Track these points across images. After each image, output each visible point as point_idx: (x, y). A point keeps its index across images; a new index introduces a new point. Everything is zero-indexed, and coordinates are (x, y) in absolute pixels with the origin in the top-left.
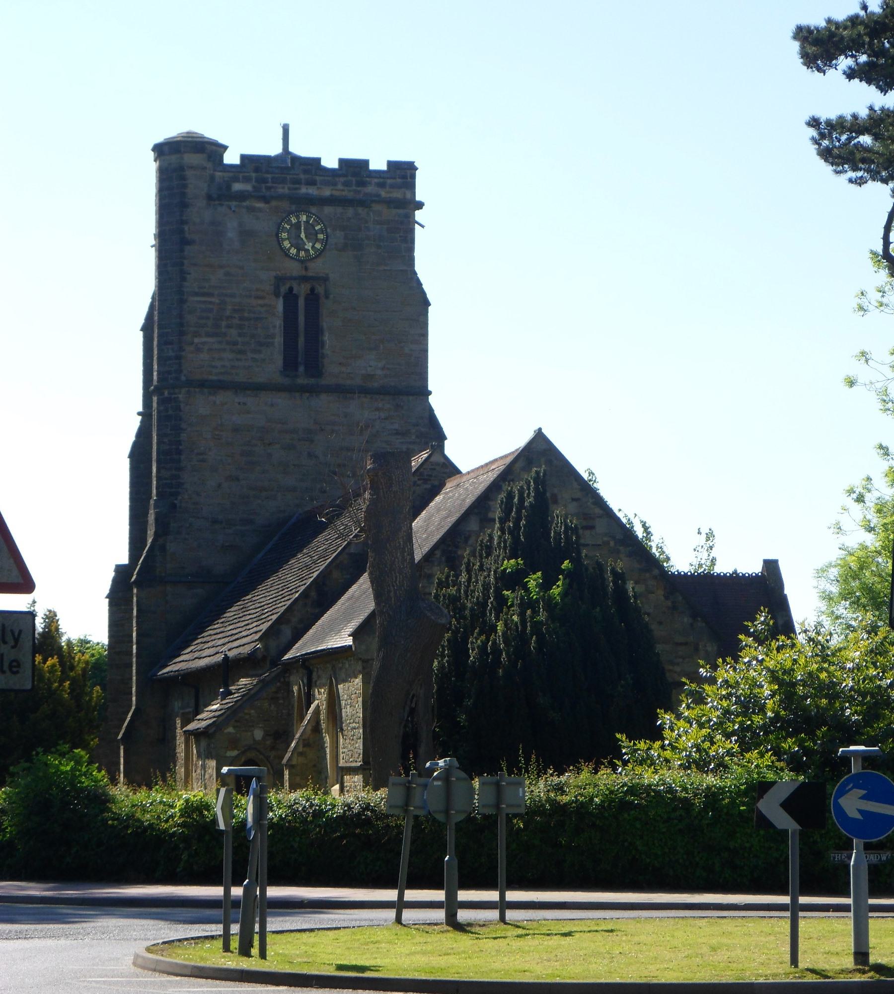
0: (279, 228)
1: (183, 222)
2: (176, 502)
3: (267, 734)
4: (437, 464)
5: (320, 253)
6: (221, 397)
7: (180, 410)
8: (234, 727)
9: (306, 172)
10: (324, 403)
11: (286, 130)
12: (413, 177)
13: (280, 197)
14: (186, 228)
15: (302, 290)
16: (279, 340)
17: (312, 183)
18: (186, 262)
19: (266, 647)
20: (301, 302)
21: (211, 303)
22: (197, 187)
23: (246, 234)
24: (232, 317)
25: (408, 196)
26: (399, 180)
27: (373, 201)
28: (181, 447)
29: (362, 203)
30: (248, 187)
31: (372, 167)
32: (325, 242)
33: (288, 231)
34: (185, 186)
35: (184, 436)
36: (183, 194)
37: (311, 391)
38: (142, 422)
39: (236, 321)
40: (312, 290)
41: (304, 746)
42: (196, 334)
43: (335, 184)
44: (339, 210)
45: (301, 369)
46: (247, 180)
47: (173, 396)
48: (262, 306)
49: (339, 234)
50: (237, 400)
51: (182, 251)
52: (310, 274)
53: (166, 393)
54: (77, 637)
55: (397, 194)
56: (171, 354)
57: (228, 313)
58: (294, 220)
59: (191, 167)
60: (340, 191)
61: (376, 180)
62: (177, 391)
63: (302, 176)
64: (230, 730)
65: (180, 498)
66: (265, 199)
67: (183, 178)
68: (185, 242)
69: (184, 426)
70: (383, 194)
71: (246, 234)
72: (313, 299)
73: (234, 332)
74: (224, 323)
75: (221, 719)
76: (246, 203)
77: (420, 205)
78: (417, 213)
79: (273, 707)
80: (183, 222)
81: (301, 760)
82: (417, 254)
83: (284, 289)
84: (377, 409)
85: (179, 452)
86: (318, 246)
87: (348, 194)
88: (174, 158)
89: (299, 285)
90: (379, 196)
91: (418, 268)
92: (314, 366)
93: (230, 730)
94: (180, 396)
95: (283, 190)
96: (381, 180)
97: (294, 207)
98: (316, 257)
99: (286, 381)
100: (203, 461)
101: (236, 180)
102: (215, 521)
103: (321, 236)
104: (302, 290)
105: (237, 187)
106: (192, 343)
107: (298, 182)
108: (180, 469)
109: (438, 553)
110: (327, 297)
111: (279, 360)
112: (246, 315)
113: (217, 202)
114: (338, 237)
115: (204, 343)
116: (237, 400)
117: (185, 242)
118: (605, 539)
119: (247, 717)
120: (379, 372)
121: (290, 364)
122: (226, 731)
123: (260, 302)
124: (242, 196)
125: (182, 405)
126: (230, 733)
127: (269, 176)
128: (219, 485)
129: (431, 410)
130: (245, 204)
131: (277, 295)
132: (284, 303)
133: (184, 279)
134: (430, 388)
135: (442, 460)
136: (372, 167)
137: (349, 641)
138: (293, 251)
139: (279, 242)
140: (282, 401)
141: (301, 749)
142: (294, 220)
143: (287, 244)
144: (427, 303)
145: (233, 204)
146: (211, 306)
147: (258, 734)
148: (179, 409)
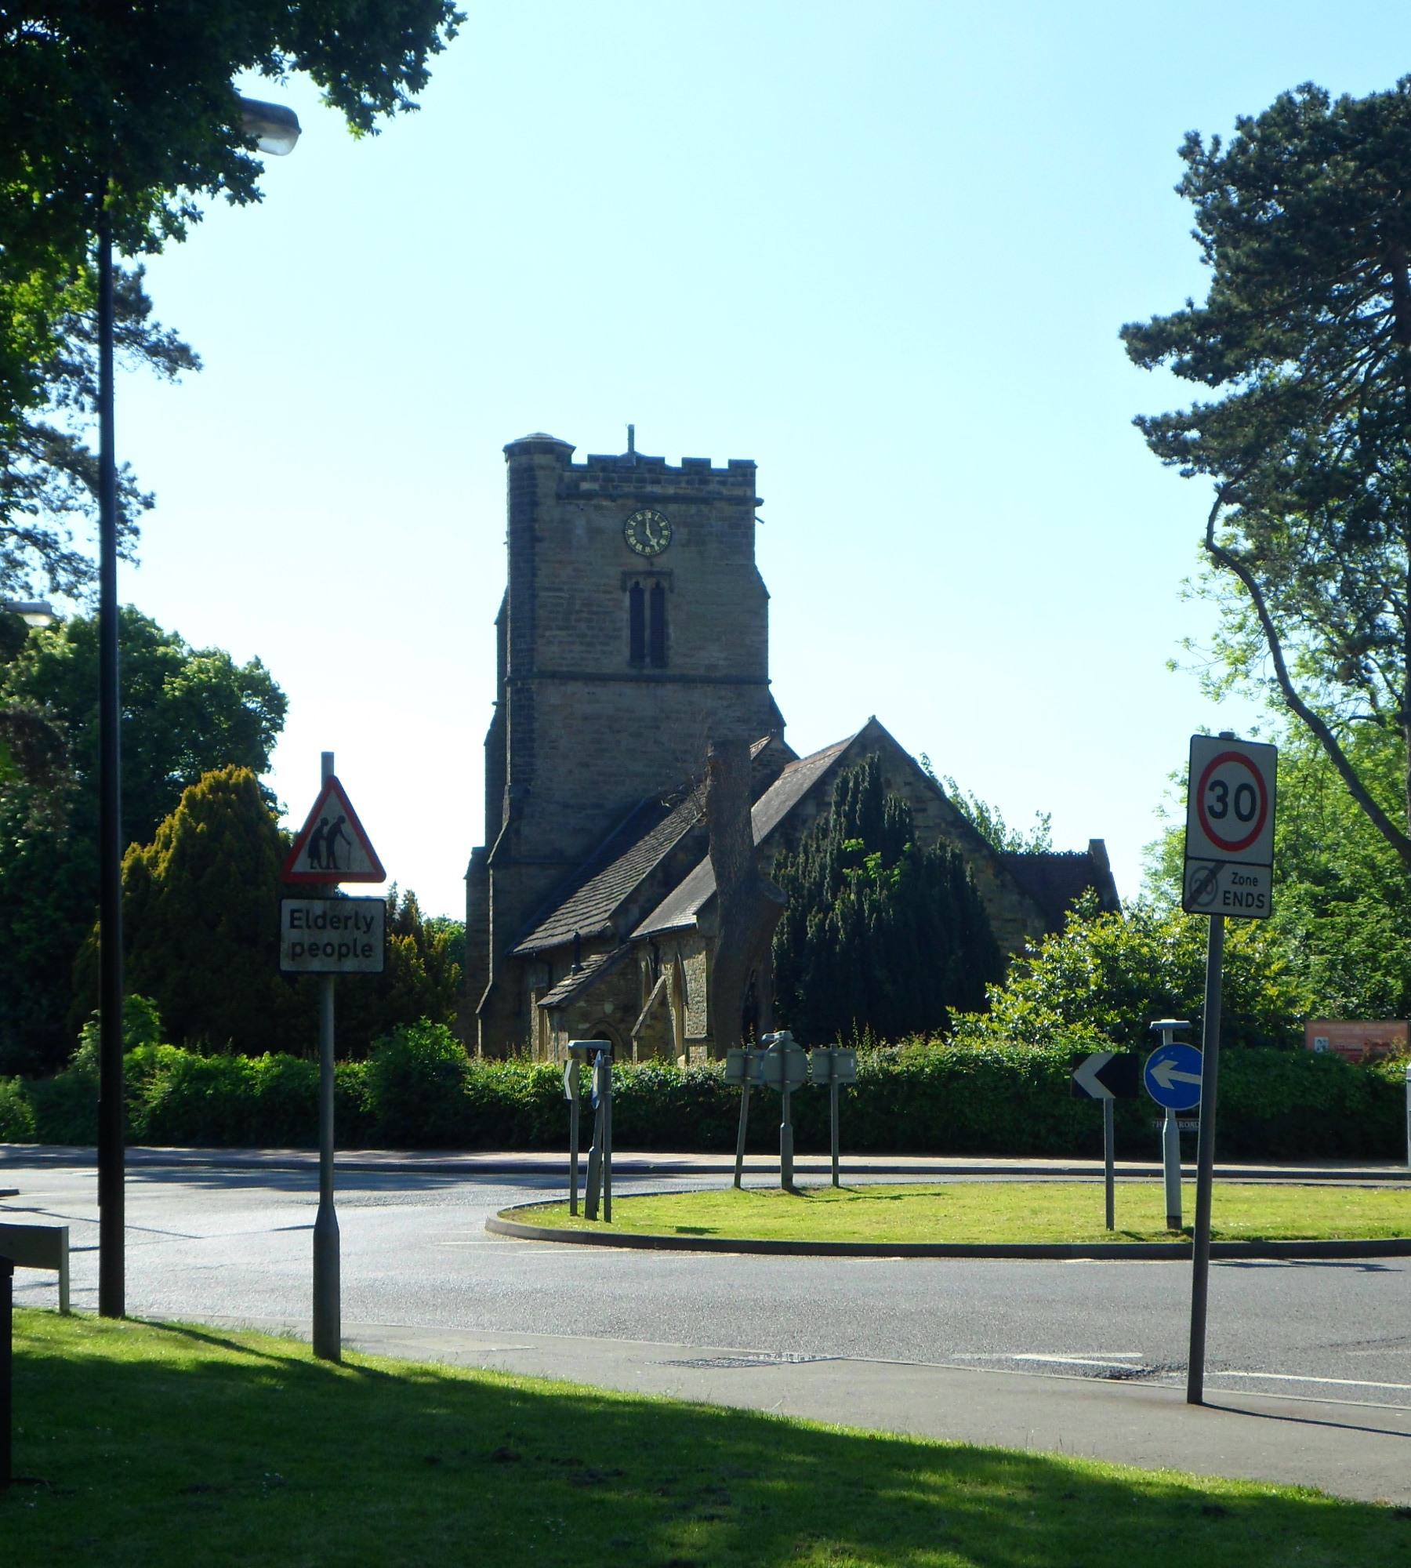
0: (625, 525)
1: (534, 520)
2: (529, 787)
3: (617, 1008)
4: (777, 750)
5: (664, 549)
6: (572, 687)
7: (533, 700)
8: (586, 1001)
9: (650, 471)
10: (671, 694)
11: (631, 431)
12: (753, 475)
13: (626, 496)
14: (537, 526)
15: (647, 584)
16: (626, 633)
17: (657, 482)
18: (537, 559)
19: (615, 925)
20: (647, 597)
21: (562, 598)
22: (547, 485)
23: (594, 532)
24: (582, 611)
25: (749, 493)
26: (740, 479)
27: (715, 499)
28: (534, 736)
29: (705, 501)
30: (595, 486)
31: (713, 466)
32: (670, 539)
33: (634, 528)
34: (535, 486)
35: (536, 725)
36: (534, 493)
37: (659, 681)
38: (496, 711)
39: (585, 615)
40: (658, 584)
41: (652, 1019)
43: (679, 483)
44: (683, 507)
45: (648, 660)
46: (594, 479)
47: (527, 687)
48: (609, 600)
49: (684, 530)
50: (586, 690)
51: (533, 548)
52: (655, 569)
53: (519, 684)
54: (436, 917)
55: (738, 492)
56: (524, 646)
57: (577, 607)
58: (639, 517)
59: (542, 467)
60: (684, 489)
61: (718, 478)
62: (530, 681)
63: (647, 476)
64: (582, 1004)
65: (533, 783)
66: (612, 498)
67: (533, 478)
68: (536, 539)
69: (536, 715)
70: (725, 491)
71: (594, 532)
72: (658, 593)
73: (583, 626)
74: (573, 617)
75: (573, 993)
76: (594, 502)
77: (760, 502)
78: (757, 509)
79: (622, 982)
80: (534, 520)
81: (650, 1032)
82: (757, 549)
83: (630, 584)
84: (721, 698)
85: (532, 740)
86: (663, 542)
87: (690, 492)
88: (524, 459)
89: (645, 579)
90: (719, 493)
91: (757, 563)
92: (660, 655)
93: (582, 1004)
94: (533, 687)
95: (629, 488)
96: (722, 479)
97: (639, 505)
98: (661, 552)
99: (634, 672)
100: (553, 748)
101: (584, 479)
103: (665, 533)
104: (647, 584)
105: (585, 486)
106: (543, 636)
107: (642, 481)
108: (532, 756)
109: (777, 835)
110: (672, 591)
111: (626, 652)
112: (595, 609)
113: (566, 501)
114: (682, 533)
116: (586, 690)
117: (536, 539)
118: (938, 821)
119: (598, 992)
120: (721, 662)
121: (637, 656)
122: (578, 1005)
123: (608, 596)
124: (589, 495)
125: (535, 697)
126: (580, 1007)
127: (614, 475)
128: (571, 772)
129: (771, 698)
130: (593, 502)
131: (624, 589)
132: (631, 600)
133: (534, 575)
134: (770, 677)
135: (782, 747)
136: (713, 466)
137: (693, 920)
138: (639, 547)
139: (626, 538)
140: (629, 690)
141: (648, 1022)
142: (639, 517)
143: (633, 541)
144: (766, 596)
145: (582, 502)
146: (562, 601)
147: (608, 1008)
148: (531, 699)
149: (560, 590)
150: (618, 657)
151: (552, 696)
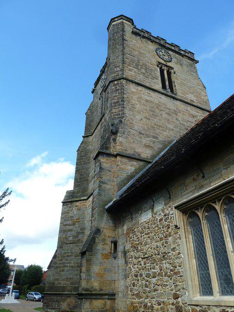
6: (140, 88)
16: (160, 79)
42: (129, 65)
72: (169, 74)
102: (140, 133)
104: (165, 69)
115: (133, 69)
121: (164, 87)
131: (158, 66)
140: (163, 97)
149: (135, 57)
150: (158, 86)
151: (132, 88)
